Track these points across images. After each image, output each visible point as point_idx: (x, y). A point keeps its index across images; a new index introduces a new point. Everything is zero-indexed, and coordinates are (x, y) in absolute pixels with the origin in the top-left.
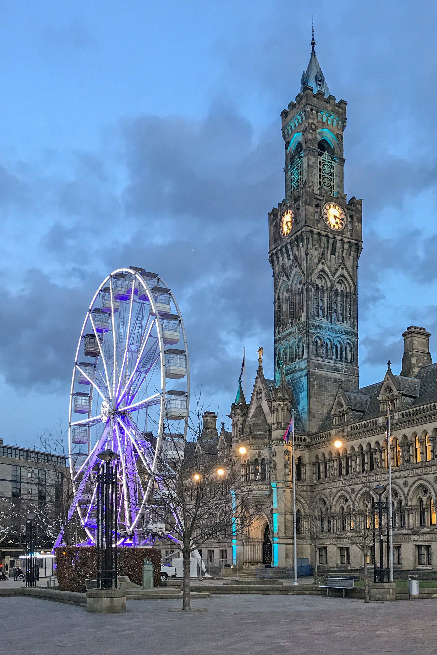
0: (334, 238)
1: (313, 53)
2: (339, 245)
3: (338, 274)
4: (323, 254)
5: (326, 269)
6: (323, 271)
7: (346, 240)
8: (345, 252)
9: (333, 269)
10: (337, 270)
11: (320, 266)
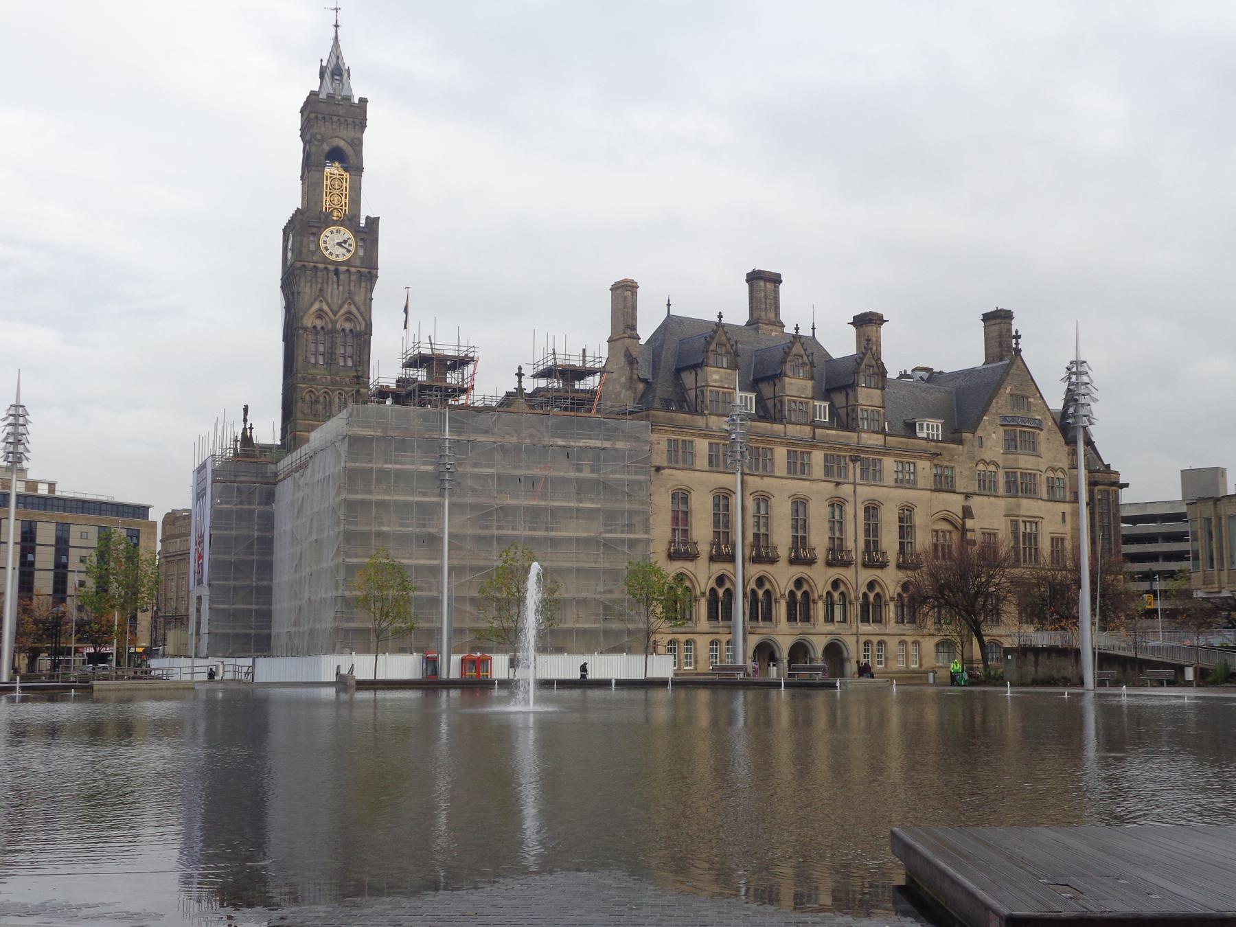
1: (336, 37)
4: (321, 290)
5: (325, 307)
6: (321, 310)
7: (353, 270)
8: (352, 284)
9: (335, 307)
10: (340, 307)
11: (316, 306)
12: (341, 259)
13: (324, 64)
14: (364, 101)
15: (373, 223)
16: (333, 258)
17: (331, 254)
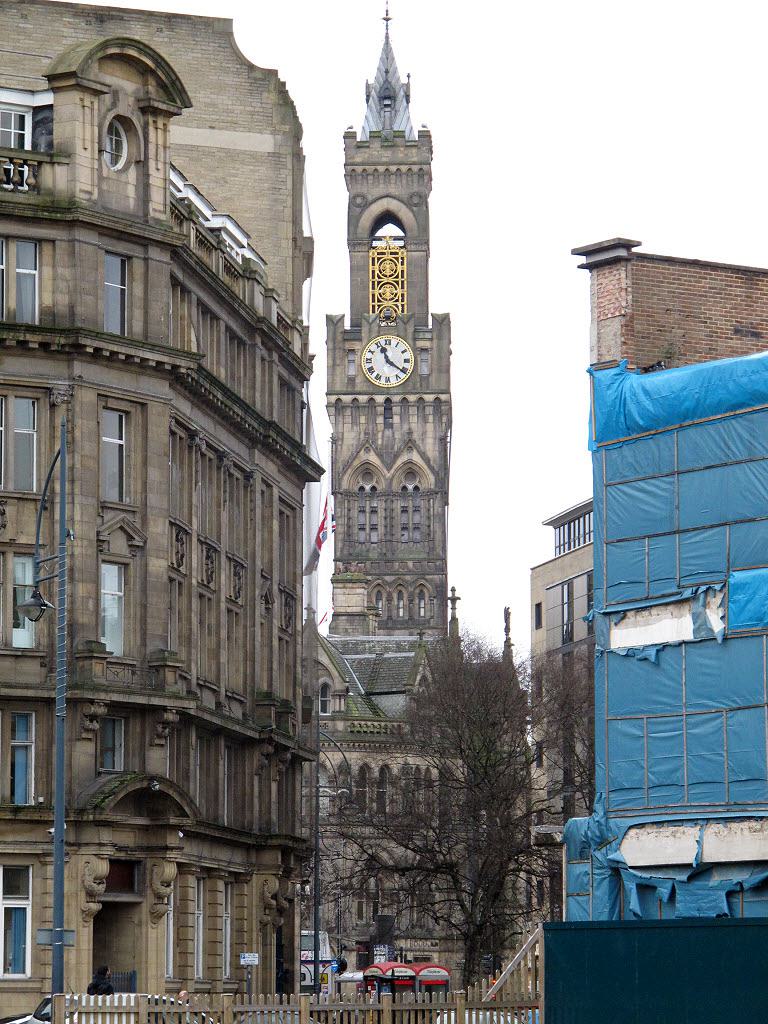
0: (388, 400)
1: (387, 37)
2: (396, 410)
3: (399, 462)
7: (412, 398)
12: (394, 382)
13: (372, 81)
14: (425, 136)
15: (443, 321)
16: (382, 383)
17: (378, 377)
